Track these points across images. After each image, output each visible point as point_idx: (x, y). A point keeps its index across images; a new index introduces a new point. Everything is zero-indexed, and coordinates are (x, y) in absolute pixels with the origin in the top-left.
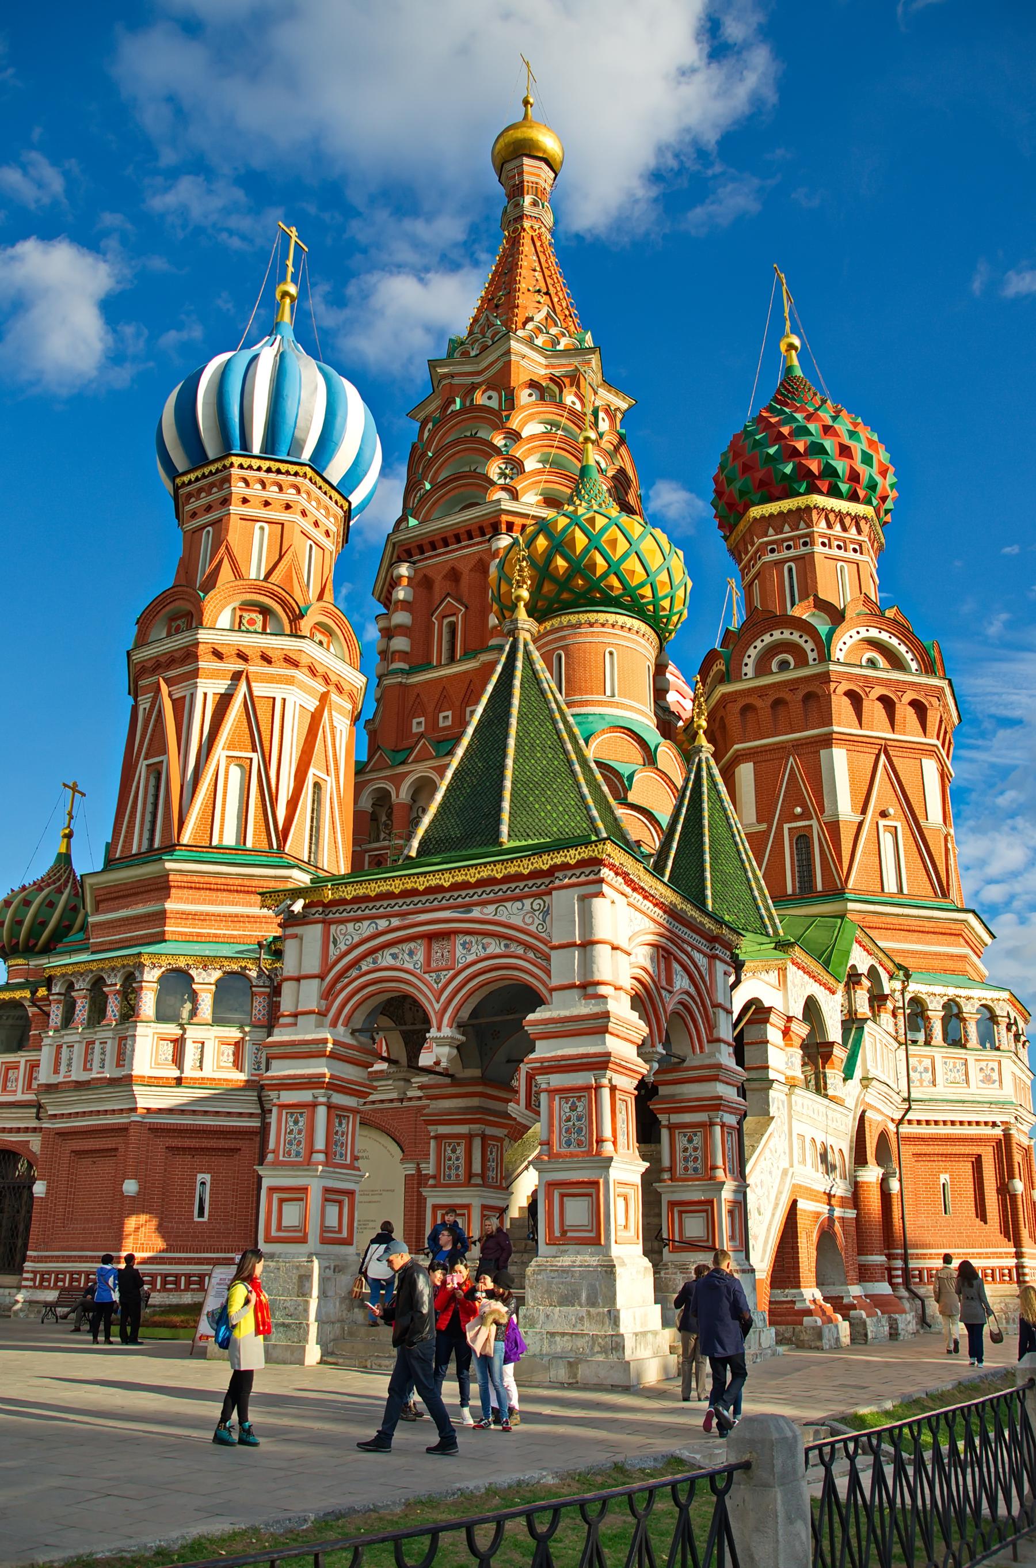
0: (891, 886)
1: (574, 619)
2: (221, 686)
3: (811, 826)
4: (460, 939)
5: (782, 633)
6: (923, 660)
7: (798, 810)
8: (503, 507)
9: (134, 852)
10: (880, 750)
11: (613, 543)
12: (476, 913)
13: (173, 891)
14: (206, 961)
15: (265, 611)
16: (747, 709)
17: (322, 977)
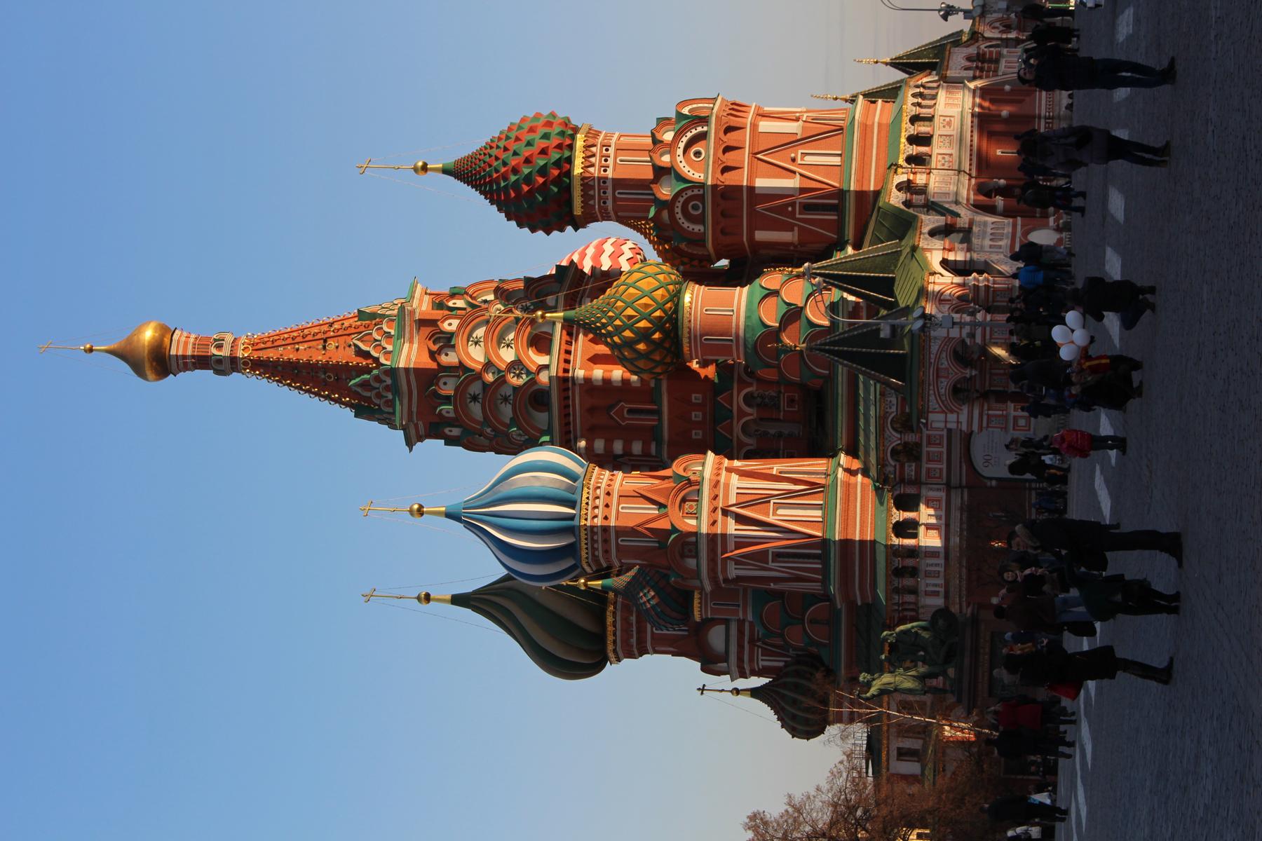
0: (837, 161)
1: (686, 331)
2: (731, 522)
3: (800, 203)
4: (940, 366)
5: (677, 207)
6: (696, 123)
7: (790, 209)
8: (555, 375)
9: (820, 566)
10: (756, 158)
11: (647, 306)
12: (932, 361)
13: (849, 537)
14: (890, 515)
15: (684, 500)
16: (723, 232)
17: (946, 413)
